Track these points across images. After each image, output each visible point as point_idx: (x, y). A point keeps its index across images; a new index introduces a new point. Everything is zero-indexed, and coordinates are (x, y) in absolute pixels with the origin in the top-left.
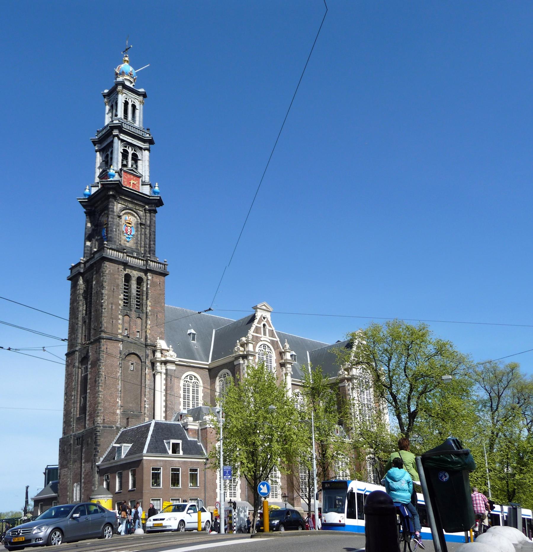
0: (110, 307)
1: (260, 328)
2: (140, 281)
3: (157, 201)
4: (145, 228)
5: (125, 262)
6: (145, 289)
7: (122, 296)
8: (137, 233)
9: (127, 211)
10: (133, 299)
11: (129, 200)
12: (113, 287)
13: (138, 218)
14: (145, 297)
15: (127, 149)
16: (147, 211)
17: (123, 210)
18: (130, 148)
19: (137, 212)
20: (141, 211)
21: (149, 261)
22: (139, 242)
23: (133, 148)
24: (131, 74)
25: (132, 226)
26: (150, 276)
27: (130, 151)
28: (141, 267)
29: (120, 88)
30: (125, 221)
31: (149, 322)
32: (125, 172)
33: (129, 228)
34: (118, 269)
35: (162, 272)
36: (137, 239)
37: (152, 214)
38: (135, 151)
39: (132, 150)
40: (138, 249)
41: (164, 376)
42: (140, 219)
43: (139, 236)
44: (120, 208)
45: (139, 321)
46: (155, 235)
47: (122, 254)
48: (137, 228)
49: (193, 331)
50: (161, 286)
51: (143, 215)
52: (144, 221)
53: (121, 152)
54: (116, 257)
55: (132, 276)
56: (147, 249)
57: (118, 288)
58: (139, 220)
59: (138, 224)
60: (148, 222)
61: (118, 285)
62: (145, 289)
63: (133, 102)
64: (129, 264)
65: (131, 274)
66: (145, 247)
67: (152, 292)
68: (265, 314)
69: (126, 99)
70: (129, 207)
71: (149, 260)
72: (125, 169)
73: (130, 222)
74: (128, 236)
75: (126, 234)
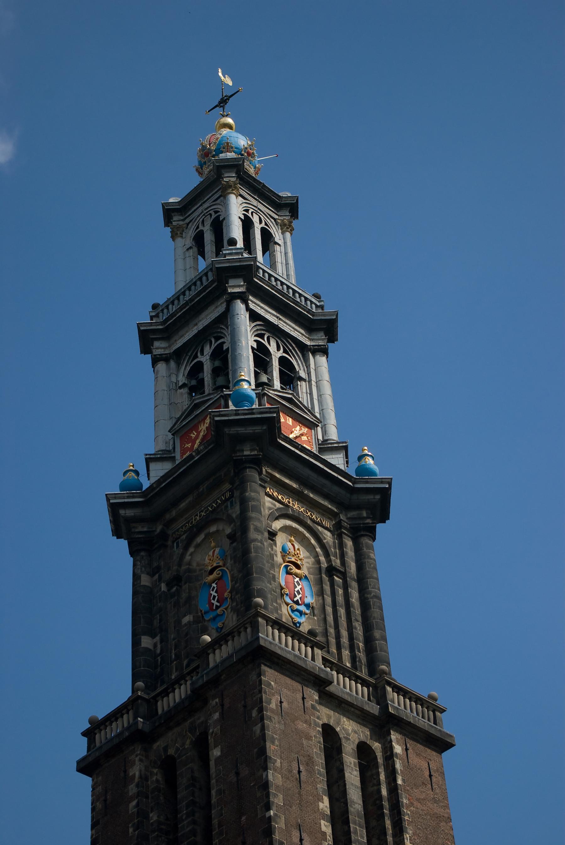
3: (378, 497)
4: (346, 587)
5: (322, 675)
6: (384, 792)
7: (325, 805)
8: (321, 601)
9: (288, 522)
10: (355, 823)
11: (295, 486)
12: (295, 764)
13: (318, 550)
14: (388, 823)
16: (345, 528)
17: (277, 518)
19: (318, 530)
20: (326, 528)
21: (389, 689)
22: (332, 631)
23: (279, 342)
24: (249, 154)
25: (306, 577)
26: (398, 743)
28: (366, 708)
29: (230, 177)
30: (283, 557)
33: (297, 579)
34: (303, 698)
35: (432, 731)
36: (325, 620)
37: (366, 541)
38: (285, 351)
39: (278, 349)
40: (333, 652)
42: (327, 555)
43: (329, 610)
44: (270, 509)
46: (381, 608)
47: (309, 650)
48: (320, 582)
50: (435, 786)
51: (334, 543)
52: (338, 561)
53: (252, 347)
54: (295, 656)
55: (341, 736)
56: (362, 656)
57: (311, 772)
58: (322, 558)
61: (310, 762)
62: (384, 792)
63: (263, 223)
64: (331, 688)
65: (338, 729)
66: (352, 648)
67: (412, 804)
69: (247, 211)
70: (293, 509)
71: (389, 684)
73: (299, 562)
74: (296, 607)
75: (288, 600)
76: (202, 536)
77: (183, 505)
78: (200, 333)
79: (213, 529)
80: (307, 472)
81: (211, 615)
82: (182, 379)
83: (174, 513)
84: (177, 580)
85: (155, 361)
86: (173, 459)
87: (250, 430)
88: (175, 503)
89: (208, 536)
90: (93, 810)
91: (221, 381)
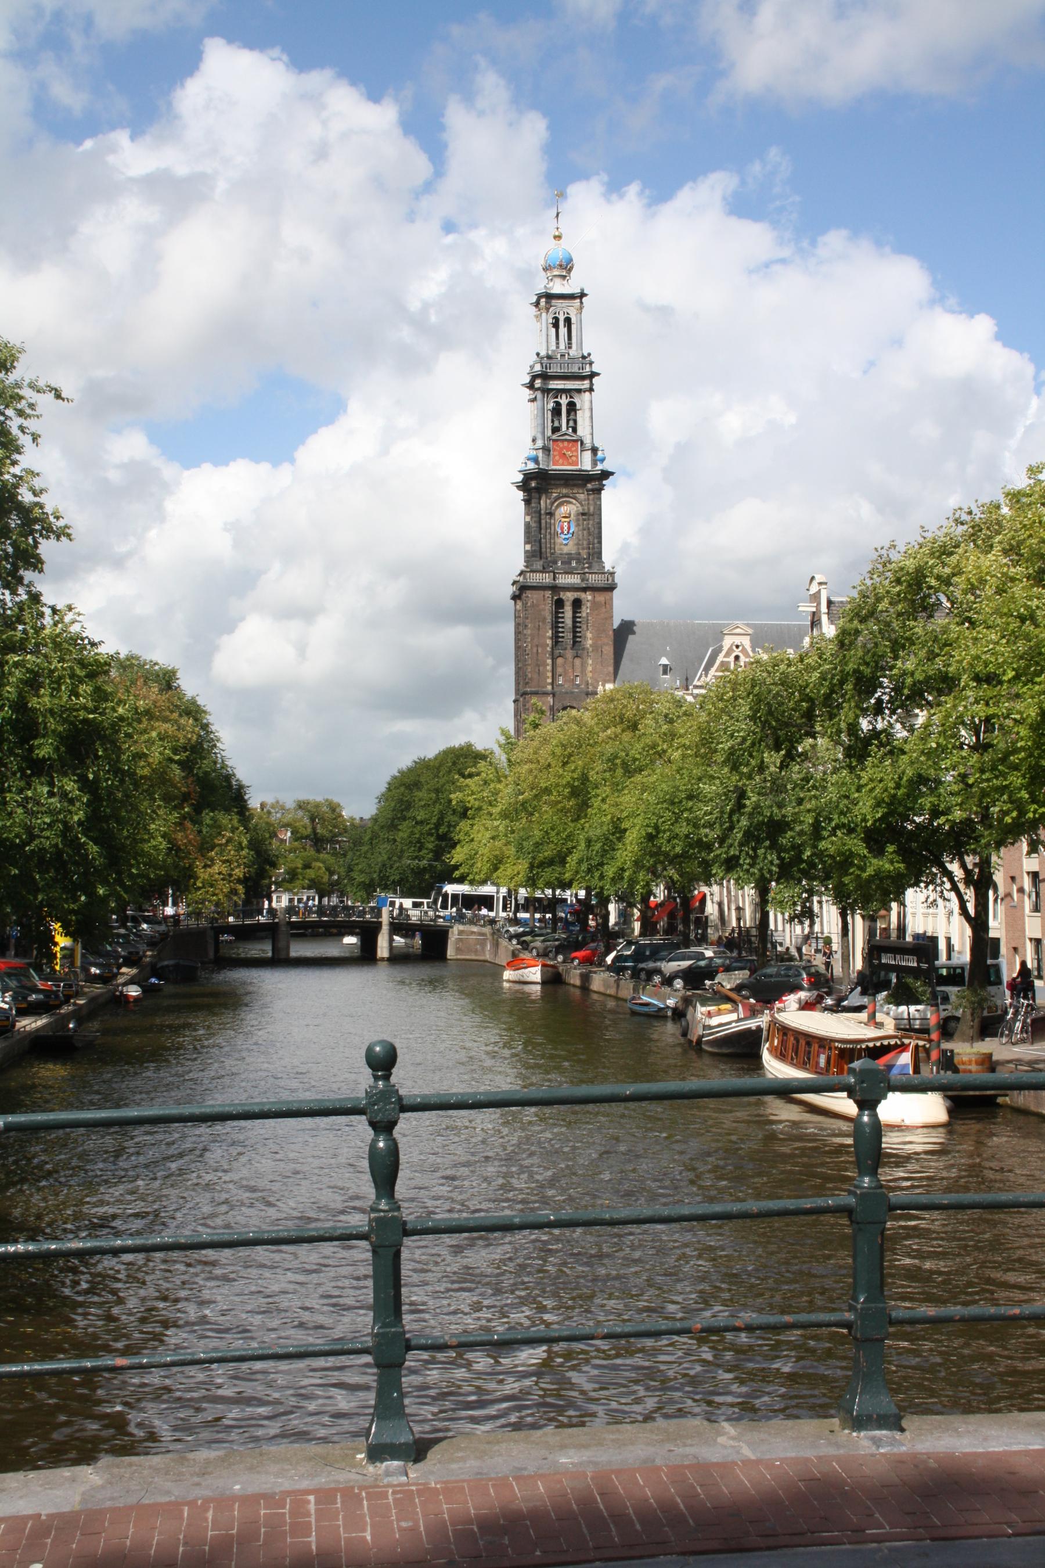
0: (535, 650)
1: (729, 662)
2: (577, 604)
6: (584, 615)
7: (550, 633)
15: (558, 400)
18: (564, 397)
27: (564, 401)
31: (590, 662)
32: (554, 441)
38: (571, 397)
45: (578, 661)
48: (578, 520)
49: (664, 661)
59: (578, 515)
60: (592, 508)
61: (545, 619)
68: (737, 640)
72: (554, 437)
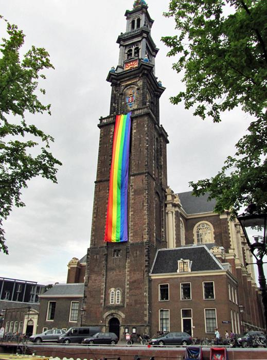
41: (174, 216)
76: (129, 87)
77: (126, 79)
78: (133, 43)
79: (132, 86)
80: (152, 81)
81: (129, 104)
82: (126, 52)
83: (123, 80)
84: (122, 94)
85: (121, 45)
86: (123, 69)
87: (148, 68)
88: (124, 78)
89: (131, 87)
90: (100, 135)
91: (137, 55)
